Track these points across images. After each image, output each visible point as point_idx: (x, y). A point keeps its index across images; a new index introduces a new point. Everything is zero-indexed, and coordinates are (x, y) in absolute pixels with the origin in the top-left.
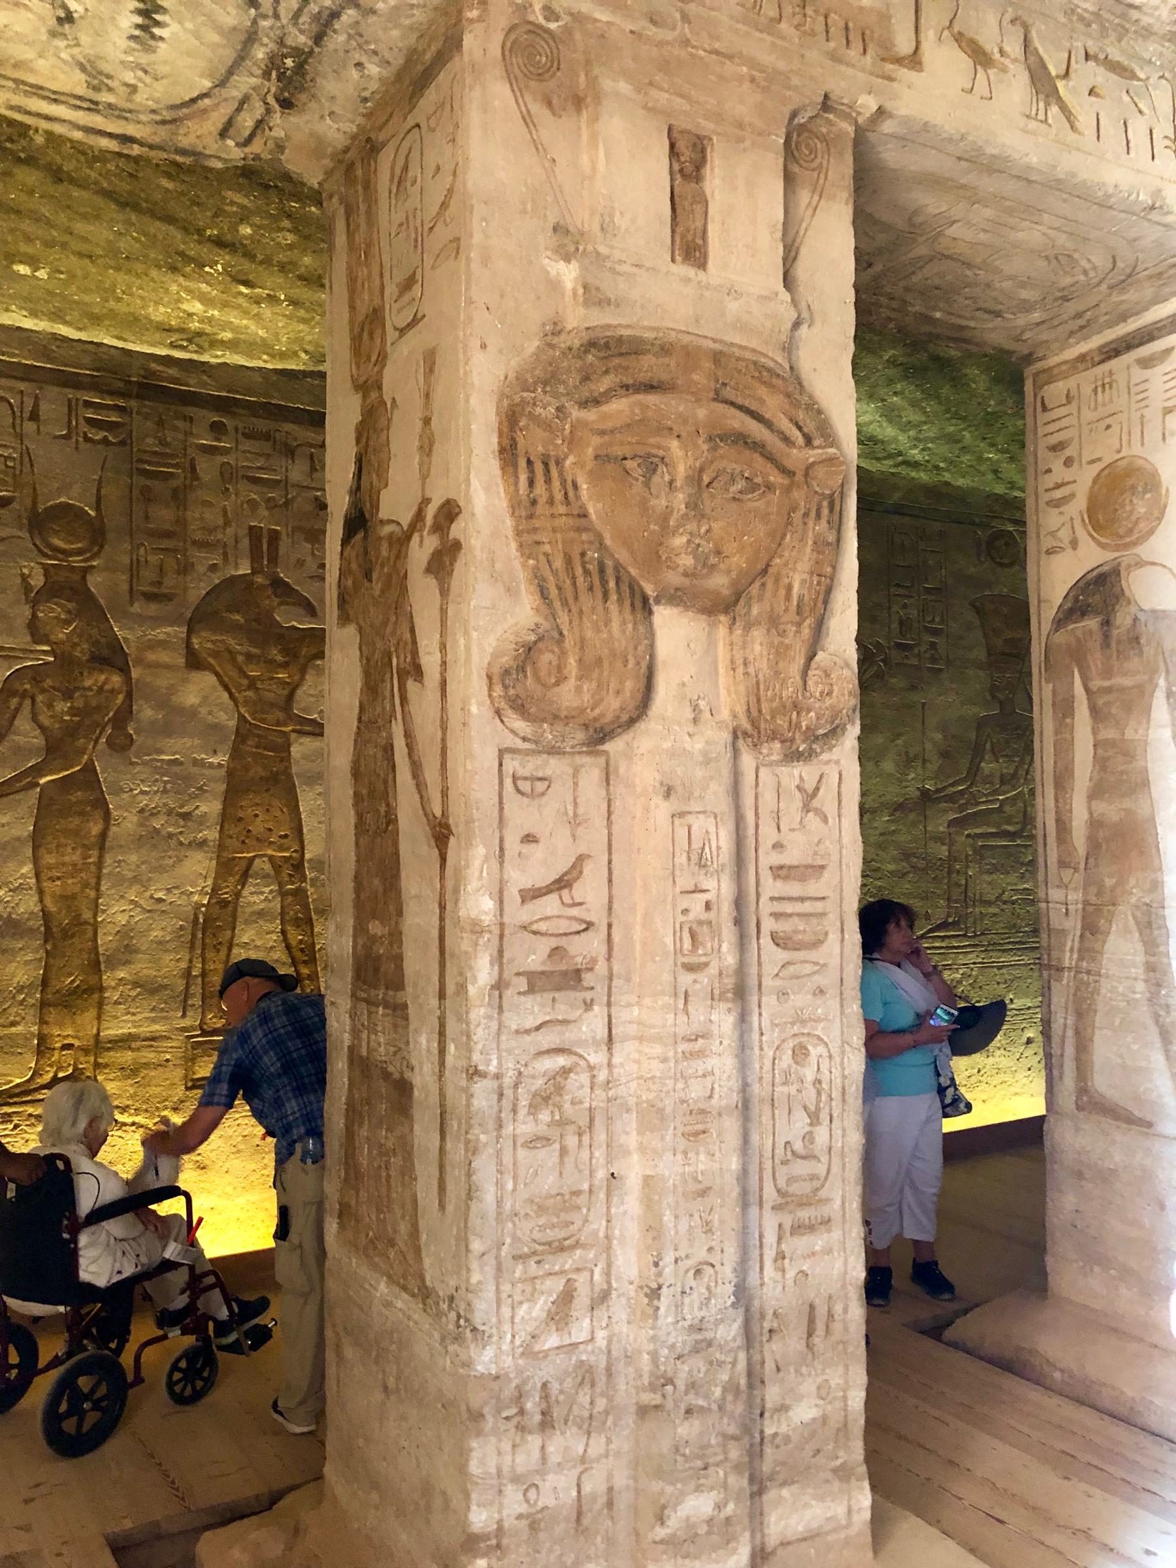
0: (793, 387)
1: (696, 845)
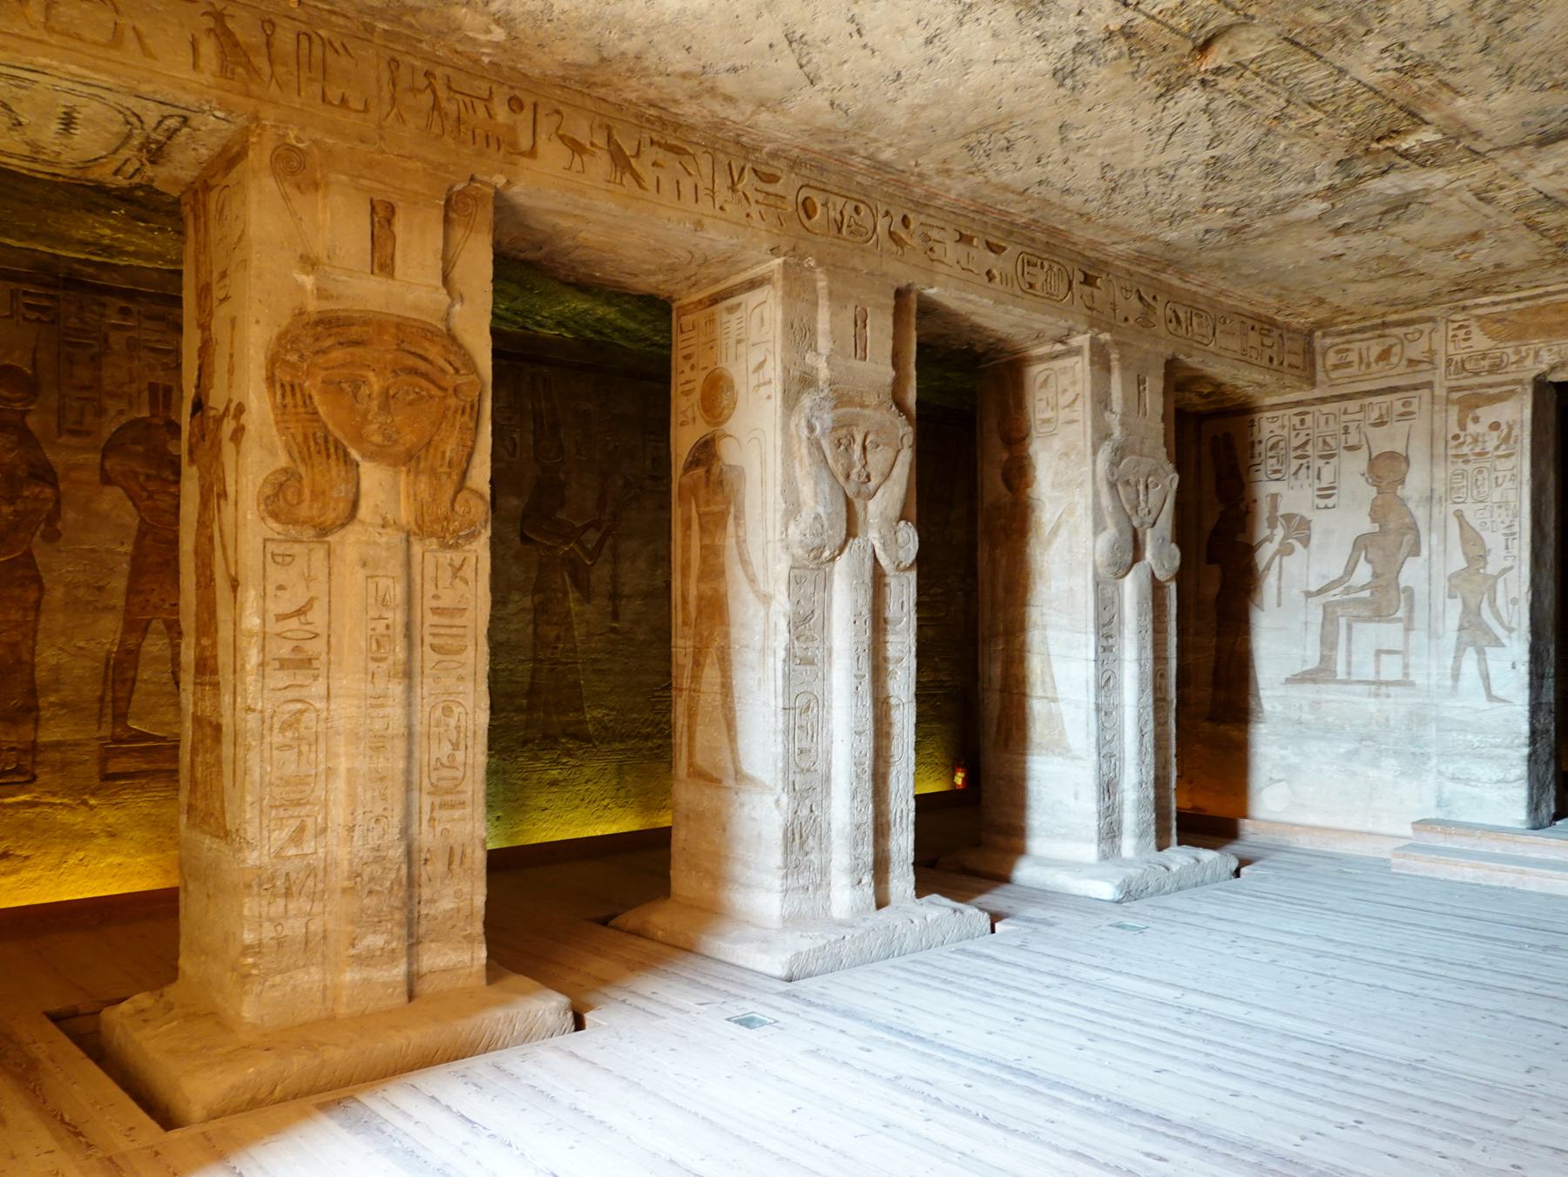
0: (451, 338)
1: (381, 593)
